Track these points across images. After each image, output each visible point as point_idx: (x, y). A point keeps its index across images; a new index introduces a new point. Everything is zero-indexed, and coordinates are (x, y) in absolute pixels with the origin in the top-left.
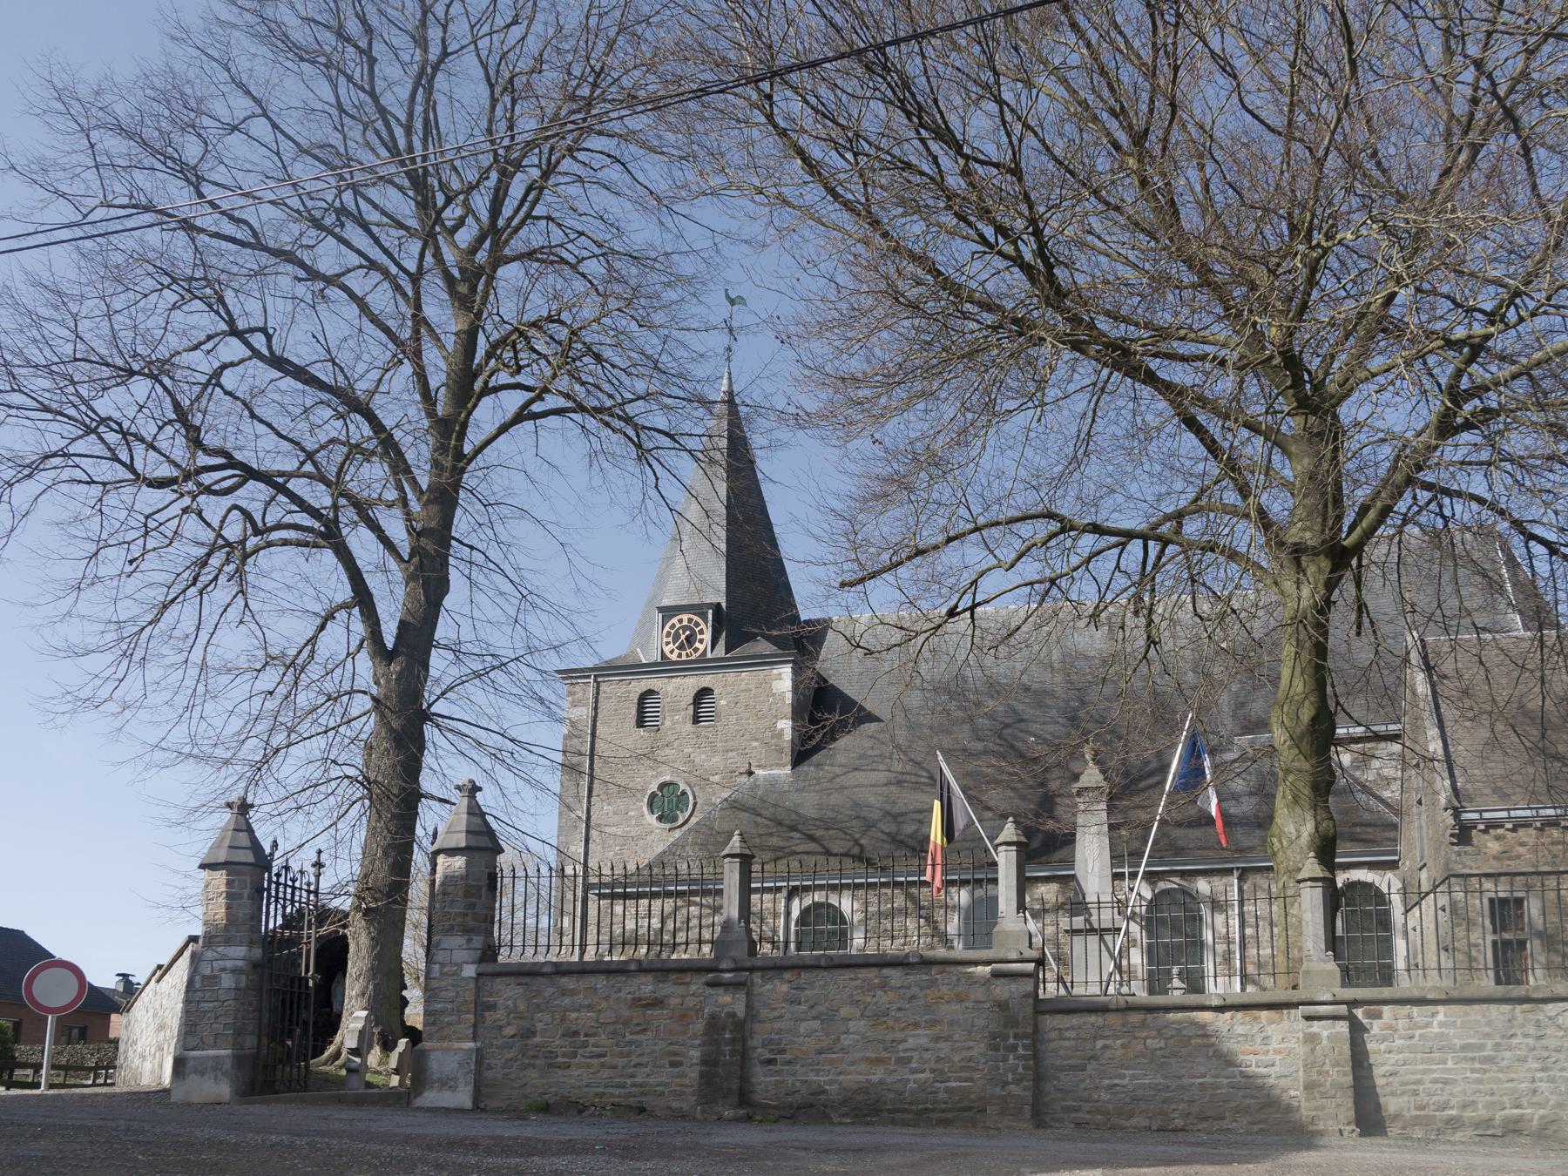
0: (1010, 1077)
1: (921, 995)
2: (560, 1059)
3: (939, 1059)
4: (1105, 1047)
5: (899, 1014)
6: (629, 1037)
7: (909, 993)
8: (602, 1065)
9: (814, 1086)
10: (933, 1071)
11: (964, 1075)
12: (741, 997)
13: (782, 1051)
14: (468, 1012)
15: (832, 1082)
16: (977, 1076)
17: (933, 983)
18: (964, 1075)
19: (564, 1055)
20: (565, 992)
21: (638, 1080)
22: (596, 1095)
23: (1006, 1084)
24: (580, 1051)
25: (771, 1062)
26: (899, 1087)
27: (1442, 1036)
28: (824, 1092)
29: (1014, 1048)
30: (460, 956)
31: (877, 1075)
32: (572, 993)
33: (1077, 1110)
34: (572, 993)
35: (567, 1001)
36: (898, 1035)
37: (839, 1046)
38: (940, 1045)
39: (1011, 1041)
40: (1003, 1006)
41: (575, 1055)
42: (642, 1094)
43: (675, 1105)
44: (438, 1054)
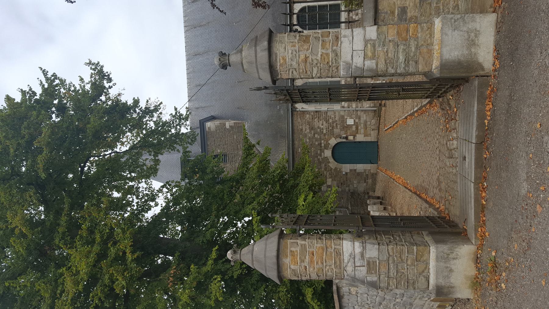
14: (407, 31)
30: (359, 45)
44: (445, 50)
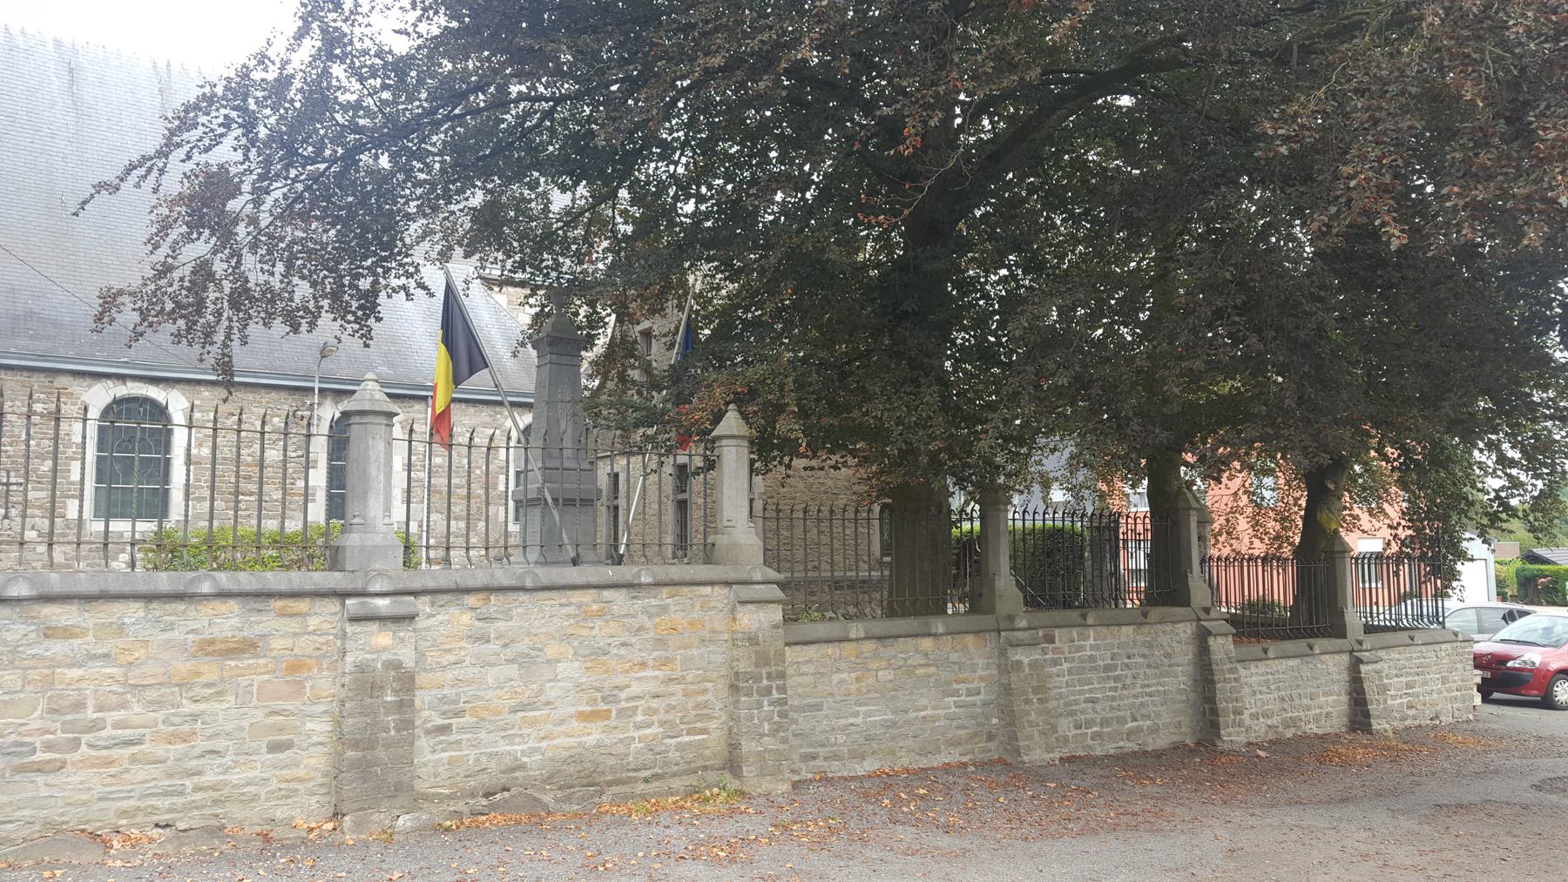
0: (766, 726)
1: (649, 624)
2: (40, 756)
3: (671, 708)
4: (841, 682)
5: (623, 651)
6: (189, 707)
7: (636, 623)
8: (134, 759)
9: (508, 760)
10: (662, 724)
11: (699, 725)
12: (405, 632)
13: (459, 714)
15: (533, 751)
16: (713, 725)
17: (664, 609)
18: (699, 725)
19: (48, 747)
20: (49, 633)
21: (208, 778)
22: (123, 813)
23: (762, 735)
24: (85, 738)
25: (444, 729)
26: (621, 749)
27: (1092, 658)
28: (522, 767)
29: (768, 691)
31: (593, 735)
32: (68, 633)
33: (814, 757)
34: (68, 633)
35: (57, 648)
36: (620, 680)
37: (543, 699)
38: (673, 688)
39: (765, 682)
40: (753, 640)
41: (75, 744)
42: (216, 802)
43: (279, 814)
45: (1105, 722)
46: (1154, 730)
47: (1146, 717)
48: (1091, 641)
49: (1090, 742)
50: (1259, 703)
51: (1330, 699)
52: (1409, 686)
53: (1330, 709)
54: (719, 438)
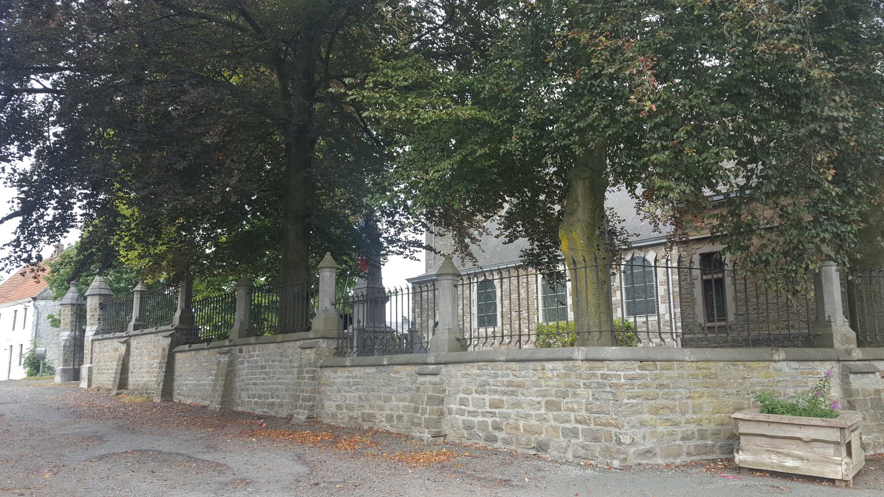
27: (256, 361)
45: (260, 397)
46: (281, 406)
47: (278, 397)
48: (257, 353)
49: (253, 406)
50: (343, 398)
51: (401, 404)
52: (494, 405)
53: (401, 413)
54: (321, 268)
